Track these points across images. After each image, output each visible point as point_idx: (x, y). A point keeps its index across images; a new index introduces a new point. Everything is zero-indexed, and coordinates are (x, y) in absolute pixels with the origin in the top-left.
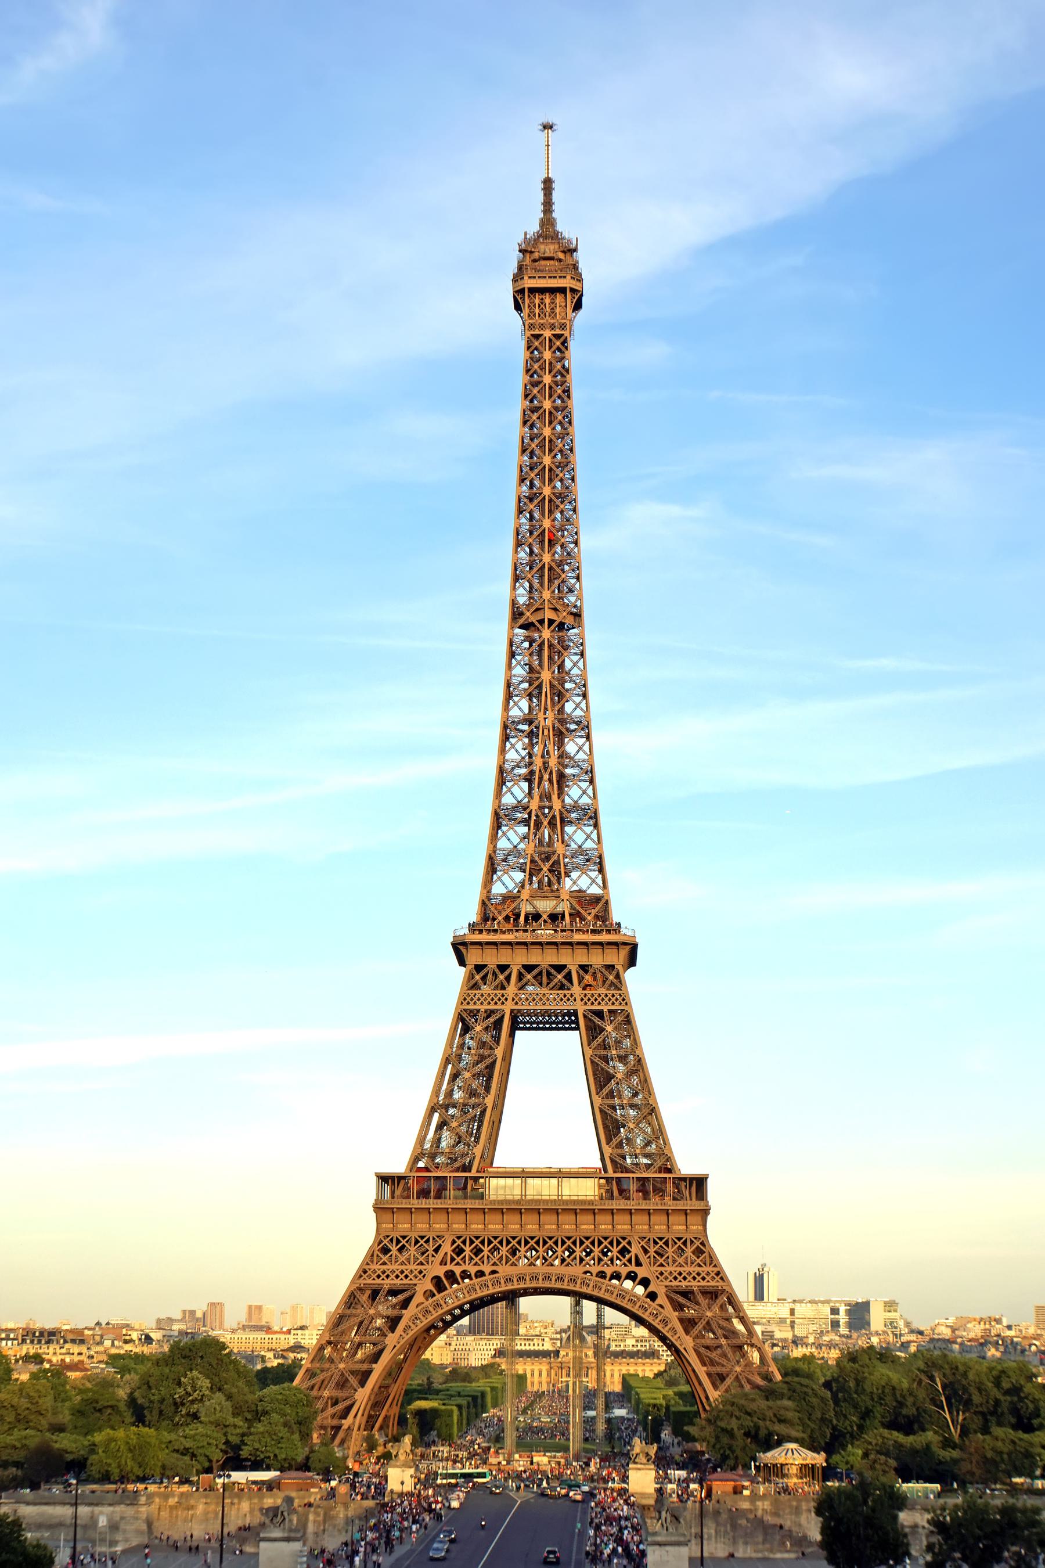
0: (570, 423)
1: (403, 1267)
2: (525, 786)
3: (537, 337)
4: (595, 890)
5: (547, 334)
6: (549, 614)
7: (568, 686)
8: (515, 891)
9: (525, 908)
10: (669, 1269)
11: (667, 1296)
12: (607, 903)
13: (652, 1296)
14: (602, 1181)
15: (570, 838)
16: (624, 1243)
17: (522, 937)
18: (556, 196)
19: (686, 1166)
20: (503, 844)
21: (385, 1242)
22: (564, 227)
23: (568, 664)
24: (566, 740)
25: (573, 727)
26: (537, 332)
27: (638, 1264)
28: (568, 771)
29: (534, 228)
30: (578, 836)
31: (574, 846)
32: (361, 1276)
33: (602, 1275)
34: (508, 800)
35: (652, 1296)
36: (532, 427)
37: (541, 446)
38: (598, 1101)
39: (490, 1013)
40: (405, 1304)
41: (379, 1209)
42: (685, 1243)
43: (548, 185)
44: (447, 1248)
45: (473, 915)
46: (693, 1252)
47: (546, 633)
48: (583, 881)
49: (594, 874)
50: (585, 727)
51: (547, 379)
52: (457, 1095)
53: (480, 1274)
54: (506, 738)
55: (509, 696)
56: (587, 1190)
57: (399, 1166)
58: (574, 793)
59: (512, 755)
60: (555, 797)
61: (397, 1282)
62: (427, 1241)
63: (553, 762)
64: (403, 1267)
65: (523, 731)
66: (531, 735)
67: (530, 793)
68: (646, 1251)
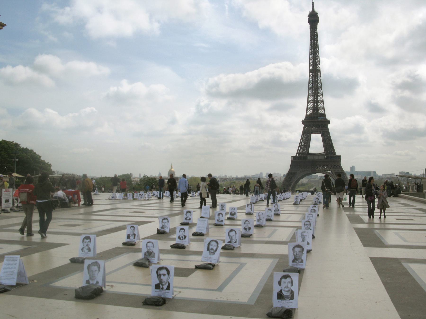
4: (323, 113)
17: (312, 120)
18: (314, 5)
19: (337, 154)
20: (309, 106)
22: (316, 10)
30: (320, 105)
34: (310, 99)
41: (292, 161)
43: (313, 3)
49: (323, 110)
50: (321, 88)
52: (303, 144)
54: (309, 90)
55: (309, 83)
56: (322, 158)
57: (294, 155)
58: (320, 98)
59: (310, 93)
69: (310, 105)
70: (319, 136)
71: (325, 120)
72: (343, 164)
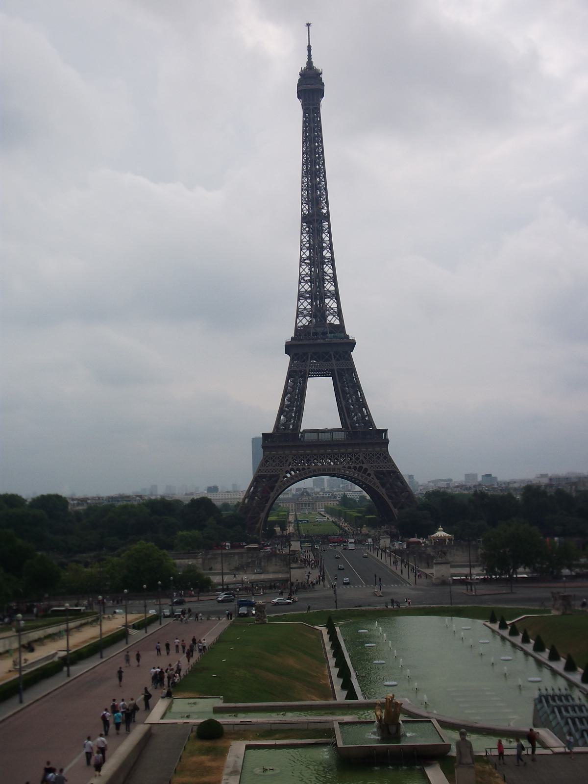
0: (322, 142)
1: (274, 468)
2: (309, 284)
3: (307, 109)
4: (337, 322)
5: (311, 107)
6: (316, 217)
7: (324, 245)
8: (307, 324)
9: (312, 331)
10: (375, 464)
11: (375, 475)
12: (344, 328)
13: (369, 475)
14: (347, 433)
15: (327, 304)
16: (357, 455)
17: (311, 342)
19: (379, 426)
21: (267, 459)
22: (316, 65)
23: (324, 236)
24: (324, 266)
25: (326, 260)
26: (307, 107)
27: (363, 463)
28: (327, 277)
29: (304, 65)
30: (331, 303)
31: (328, 306)
32: (258, 472)
33: (349, 468)
34: (303, 290)
35: (369, 475)
36: (306, 145)
37: (310, 151)
38: (344, 403)
39: (301, 371)
40: (276, 481)
41: (263, 447)
42: (380, 455)
43: (309, 48)
44: (290, 460)
45: (291, 334)
46: (384, 458)
47: (316, 225)
48: (333, 320)
51: (312, 125)
52: (286, 402)
53: (303, 469)
55: (301, 249)
56: (341, 436)
58: (329, 286)
60: (322, 288)
61: (273, 473)
62: (283, 458)
63: (320, 275)
64: (274, 468)
65: (307, 263)
66: (310, 264)
67: (311, 286)
68: (366, 458)
69: (306, 304)
70: (327, 383)
71: (345, 340)
72: (394, 451)
